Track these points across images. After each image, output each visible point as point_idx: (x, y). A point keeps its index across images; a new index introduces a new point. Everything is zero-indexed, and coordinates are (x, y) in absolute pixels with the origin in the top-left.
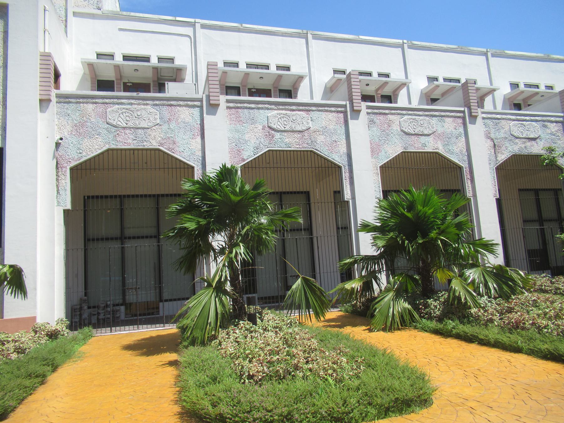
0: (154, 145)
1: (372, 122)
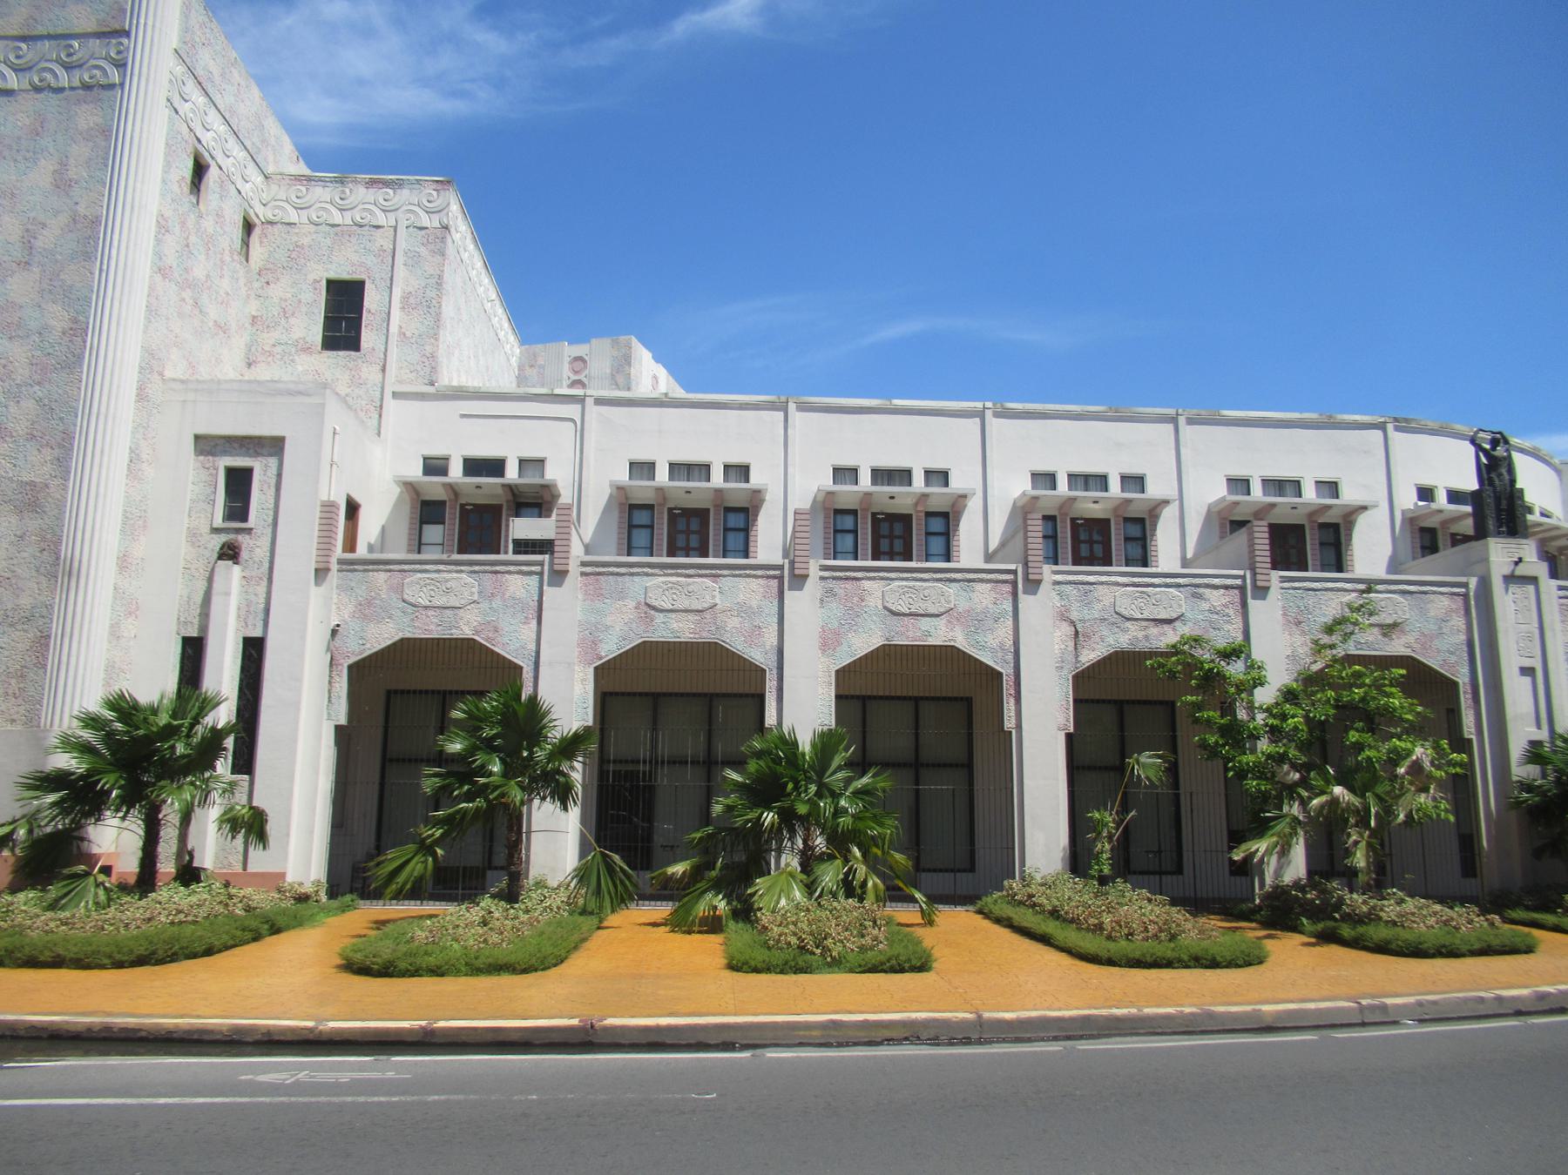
0: (466, 632)
1: (830, 592)
